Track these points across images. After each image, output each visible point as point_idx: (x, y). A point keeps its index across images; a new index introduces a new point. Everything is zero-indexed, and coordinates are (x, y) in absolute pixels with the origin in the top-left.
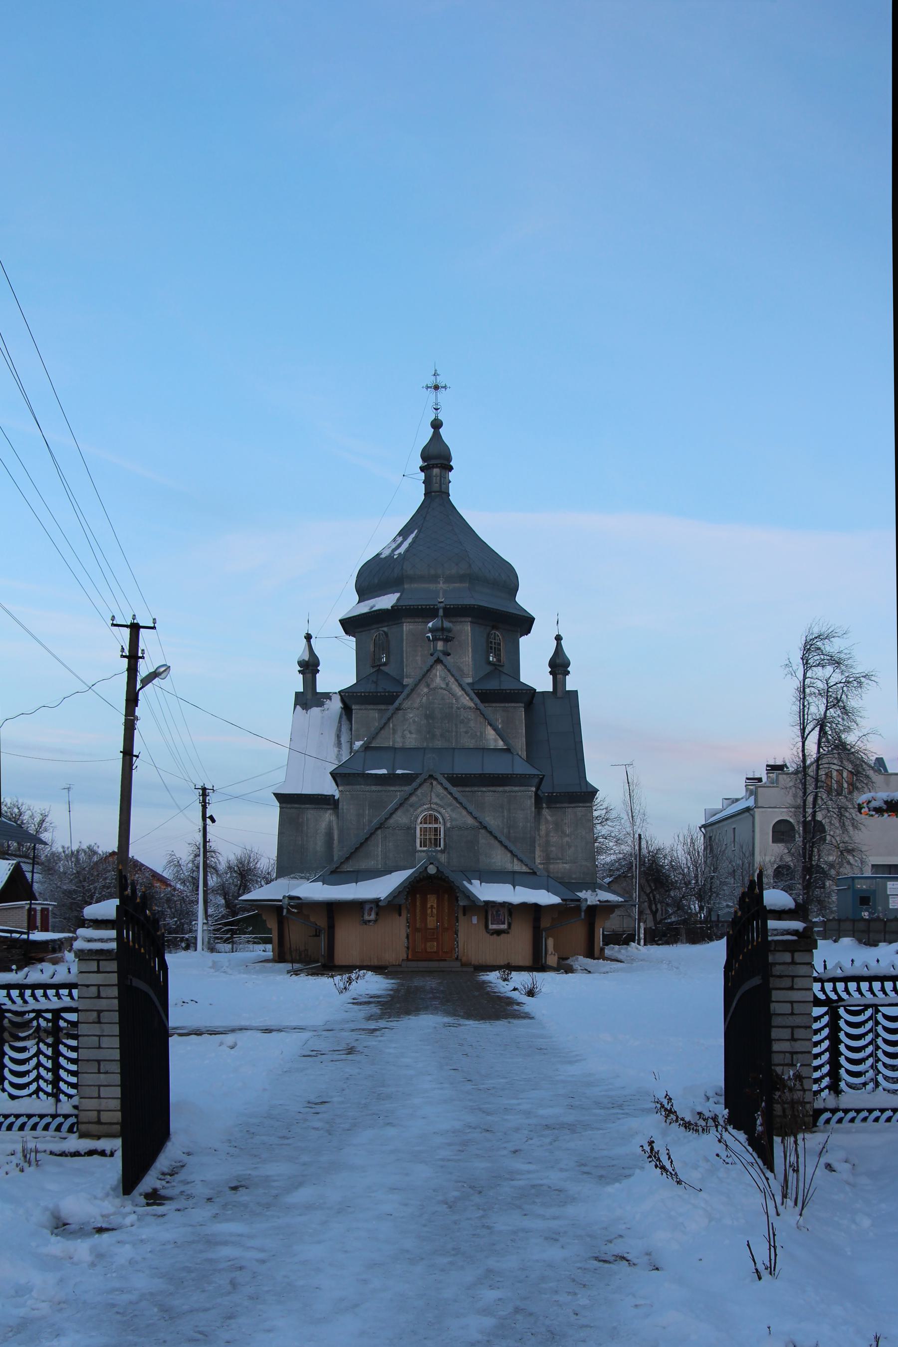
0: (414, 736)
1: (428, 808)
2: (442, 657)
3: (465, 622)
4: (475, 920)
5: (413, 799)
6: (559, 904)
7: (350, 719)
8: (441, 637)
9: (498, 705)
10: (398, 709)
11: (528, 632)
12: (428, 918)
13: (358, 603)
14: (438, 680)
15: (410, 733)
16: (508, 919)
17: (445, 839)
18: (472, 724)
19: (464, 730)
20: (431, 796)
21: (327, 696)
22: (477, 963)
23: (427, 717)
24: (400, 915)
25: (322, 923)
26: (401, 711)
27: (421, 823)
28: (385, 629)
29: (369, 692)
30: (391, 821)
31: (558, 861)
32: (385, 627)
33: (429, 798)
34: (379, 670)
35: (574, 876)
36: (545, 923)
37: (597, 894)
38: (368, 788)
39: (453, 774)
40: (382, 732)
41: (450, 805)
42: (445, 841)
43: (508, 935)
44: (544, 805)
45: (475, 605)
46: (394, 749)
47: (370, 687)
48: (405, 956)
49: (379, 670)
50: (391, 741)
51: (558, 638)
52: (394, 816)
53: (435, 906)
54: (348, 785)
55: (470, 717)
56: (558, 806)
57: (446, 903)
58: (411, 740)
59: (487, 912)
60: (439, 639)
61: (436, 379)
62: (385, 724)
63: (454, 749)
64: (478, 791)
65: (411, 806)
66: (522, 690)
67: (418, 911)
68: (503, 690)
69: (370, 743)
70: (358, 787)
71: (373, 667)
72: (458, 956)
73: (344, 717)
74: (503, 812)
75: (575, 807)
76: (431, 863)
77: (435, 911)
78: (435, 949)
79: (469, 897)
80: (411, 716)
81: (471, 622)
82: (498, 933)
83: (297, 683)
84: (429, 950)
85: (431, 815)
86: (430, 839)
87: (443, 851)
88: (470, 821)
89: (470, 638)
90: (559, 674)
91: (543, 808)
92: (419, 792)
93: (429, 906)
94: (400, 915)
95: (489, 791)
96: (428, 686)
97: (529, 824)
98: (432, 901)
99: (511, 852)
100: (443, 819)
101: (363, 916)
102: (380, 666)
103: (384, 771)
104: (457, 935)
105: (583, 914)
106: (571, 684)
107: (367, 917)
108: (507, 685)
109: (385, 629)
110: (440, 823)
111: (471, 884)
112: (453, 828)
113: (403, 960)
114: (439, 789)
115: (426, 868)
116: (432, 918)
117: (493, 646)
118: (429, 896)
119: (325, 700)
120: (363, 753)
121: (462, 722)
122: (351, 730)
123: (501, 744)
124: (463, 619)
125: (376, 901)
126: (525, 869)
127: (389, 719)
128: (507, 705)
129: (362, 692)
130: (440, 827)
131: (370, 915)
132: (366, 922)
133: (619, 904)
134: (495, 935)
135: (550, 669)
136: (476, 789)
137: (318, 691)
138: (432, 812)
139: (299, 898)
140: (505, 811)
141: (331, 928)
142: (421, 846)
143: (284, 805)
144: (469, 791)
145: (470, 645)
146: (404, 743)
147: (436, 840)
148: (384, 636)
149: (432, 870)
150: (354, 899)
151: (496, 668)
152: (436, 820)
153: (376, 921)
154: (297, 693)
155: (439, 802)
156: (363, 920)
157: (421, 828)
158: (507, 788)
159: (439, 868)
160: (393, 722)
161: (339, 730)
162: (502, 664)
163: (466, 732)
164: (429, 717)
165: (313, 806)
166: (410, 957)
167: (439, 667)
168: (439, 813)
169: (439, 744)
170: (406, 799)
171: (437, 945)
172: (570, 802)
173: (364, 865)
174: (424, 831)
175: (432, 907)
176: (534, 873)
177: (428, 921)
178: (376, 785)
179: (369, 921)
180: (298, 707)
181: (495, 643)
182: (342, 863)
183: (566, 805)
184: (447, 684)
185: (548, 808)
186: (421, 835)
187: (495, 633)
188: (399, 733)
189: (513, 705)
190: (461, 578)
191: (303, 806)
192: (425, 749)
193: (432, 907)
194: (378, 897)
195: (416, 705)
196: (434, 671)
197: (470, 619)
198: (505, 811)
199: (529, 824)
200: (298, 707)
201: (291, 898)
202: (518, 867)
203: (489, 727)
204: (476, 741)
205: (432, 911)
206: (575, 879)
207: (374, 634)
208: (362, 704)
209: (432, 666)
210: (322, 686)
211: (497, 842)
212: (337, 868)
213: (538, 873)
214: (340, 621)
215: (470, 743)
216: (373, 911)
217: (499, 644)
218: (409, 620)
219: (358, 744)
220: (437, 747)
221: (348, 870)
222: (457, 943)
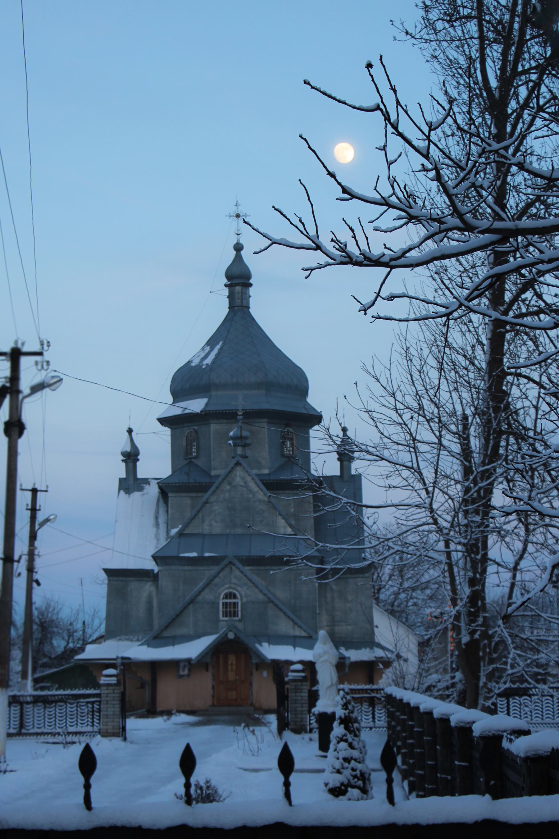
0: (219, 524)
2: (241, 460)
4: (265, 674)
5: (217, 580)
7: (166, 501)
10: (206, 503)
14: (238, 479)
15: (216, 522)
21: (146, 481)
24: (207, 670)
25: (147, 677)
27: (223, 599)
29: (183, 483)
30: (200, 598)
38: (181, 568)
46: (203, 535)
47: (182, 479)
48: (211, 703)
49: (190, 462)
52: (202, 593)
53: (234, 663)
58: (218, 528)
60: (239, 446)
62: (196, 515)
69: (184, 530)
70: (174, 567)
71: (186, 459)
73: (161, 501)
76: (231, 631)
77: (234, 667)
85: (231, 593)
87: (240, 621)
88: (261, 597)
92: (221, 575)
93: (230, 663)
94: (207, 670)
96: (230, 484)
98: (232, 659)
99: (293, 621)
100: (241, 596)
101: (178, 671)
102: (191, 458)
103: (194, 554)
107: (181, 673)
111: (261, 645)
114: (237, 573)
115: (226, 635)
119: (144, 485)
122: (167, 512)
125: (189, 661)
126: (304, 634)
127: (198, 511)
129: (176, 483)
132: (181, 677)
137: (139, 476)
139: (129, 659)
141: (154, 681)
142: (223, 616)
149: (231, 636)
152: (235, 597)
153: (188, 675)
154: (121, 480)
157: (223, 603)
161: (157, 512)
163: (262, 521)
166: (215, 703)
167: (239, 468)
169: (239, 531)
170: (212, 580)
174: (225, 605)
175: (232, 664)
178: (188, 565)
179: (183, 676)
180: (122, 492)
182: (162, 631)
184: (246, 483)
186: (223, 608)
188: (207, 522)
192: (227, 535)
193: (232, 664)
201: (123, 658)
202: (298, 632)
203: (279, 517)
205: (232, 667)
208: (177, 492)
209: (233, 468)
210: (141, 474)
212: (158, 634)
219: (174, 531)
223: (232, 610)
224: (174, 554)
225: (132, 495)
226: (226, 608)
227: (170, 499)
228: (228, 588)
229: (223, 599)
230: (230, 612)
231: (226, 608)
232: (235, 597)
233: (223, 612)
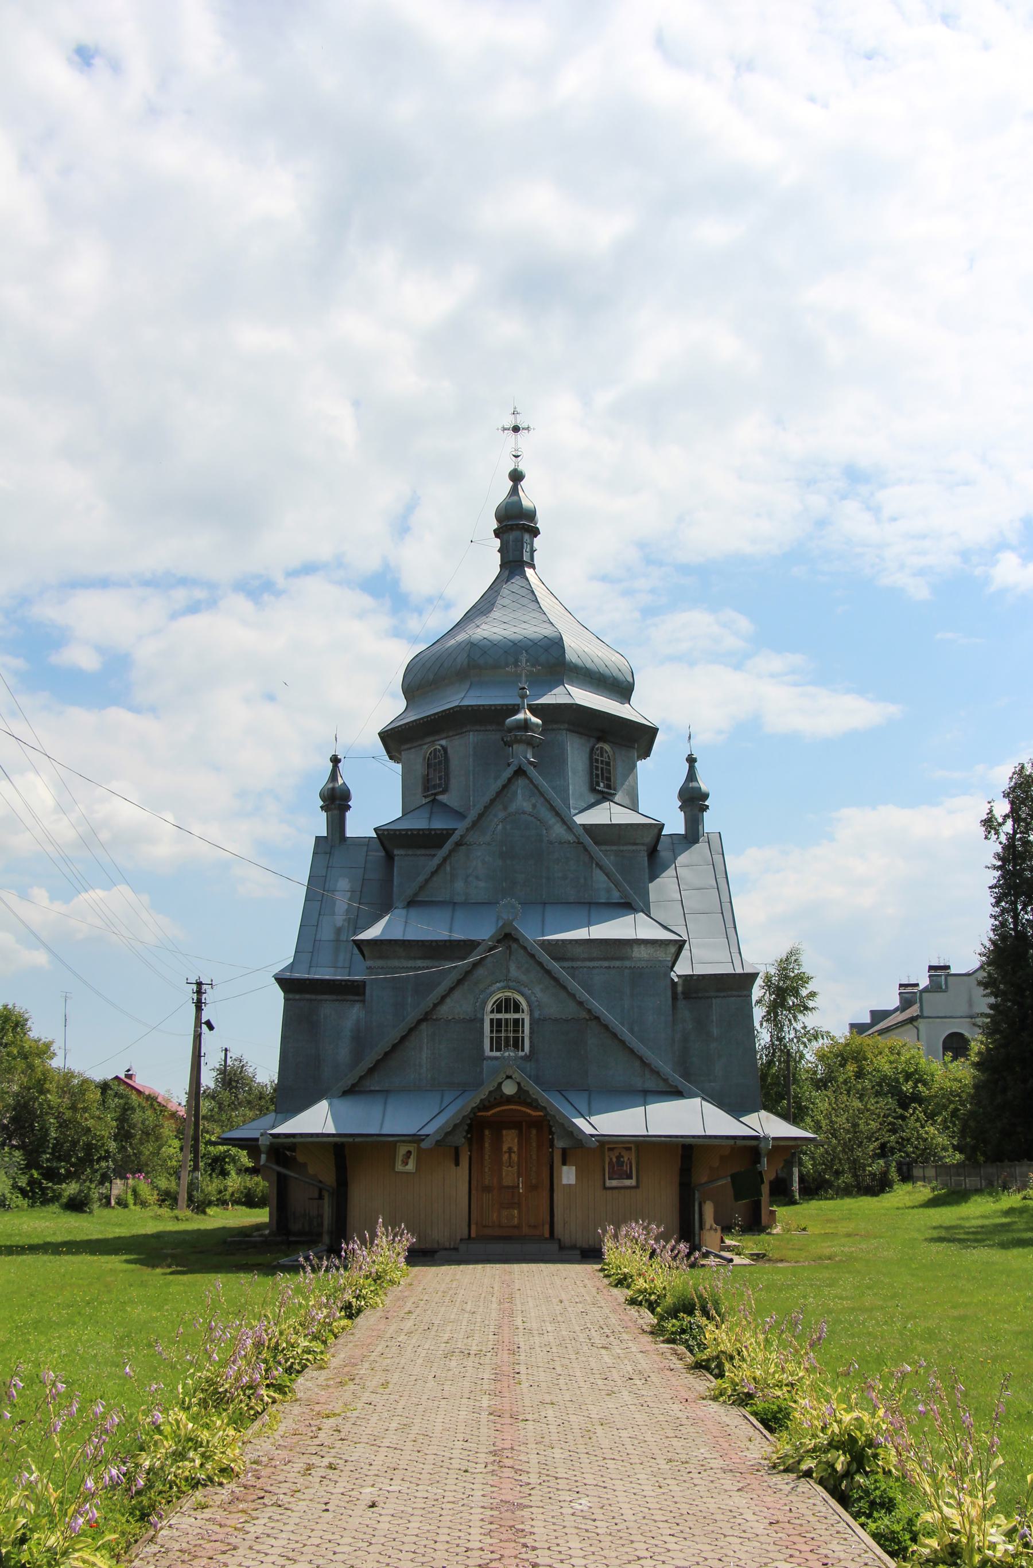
0: (482, 884)
11: (646, 753)
17: (531, 1038)
22: (585, 1246)
24: (457, 1164)
27: (492, 1012)
28: (443, 742)
30: (444, 1010)
32: (442, 739)
34: (434, 801)
40: (435, 879)
42: (531, 1042)
48: (465, 1235)
49: (434, 801)
51: (691, 760)
52: (448, 1000)
53: (515, 1149)
57: (534, 1144)
61: (516, 419)
71: (425, 797)
75: (724, 997)
76: (509, 1077)
77: (515, 1157)
78: (516, 1221)
79: (572, 1133)
81: (567, 730)
83: (319, 824)
85: (507, 1000)
86: (507, 1038)
87: (526, 1058)
93: (505, 1148)
94: (457, 1164)
100: (529, 1005)
106: (710, 822)
109: (443, 742)
110: (523, 1012)
112: (545, 1020)
113: (461, 1240)
115: (500, 1084)
117: (600, 765)
118: (504, 1132)
124: (555, 726)
130: (523, 1019)
131: (407, 1164)
137: (348, 834)
142: (491, 1050)
143: (291, 996)
147: (516, 1039)
148: (442, 752)
152: (517, 1008)
154: (318, 839)
157: (492, 1020)
159: (522, 1085)
160: (450, 863)
165: (334, 997)
166: (473, 1235)
167: (521, 782)
168: (523, 995)
171: (520, 1213)
174: (496, 1025)
175: (510, 1151)
177: (504, 1174)
185: (684, 998)
186: (492, 1031)
191: (319, 997)
193: (510, 1151)
205: (510, 1157)
207: (427, 750)
212: (353, 1086)
216: (412, 1157)
218: (478, 728)
221: (373, 1088)
227: (396, 858)
229: (492, 1012)
230: (507, 1038)
231: (499, 1031)
233: (492, 1038)
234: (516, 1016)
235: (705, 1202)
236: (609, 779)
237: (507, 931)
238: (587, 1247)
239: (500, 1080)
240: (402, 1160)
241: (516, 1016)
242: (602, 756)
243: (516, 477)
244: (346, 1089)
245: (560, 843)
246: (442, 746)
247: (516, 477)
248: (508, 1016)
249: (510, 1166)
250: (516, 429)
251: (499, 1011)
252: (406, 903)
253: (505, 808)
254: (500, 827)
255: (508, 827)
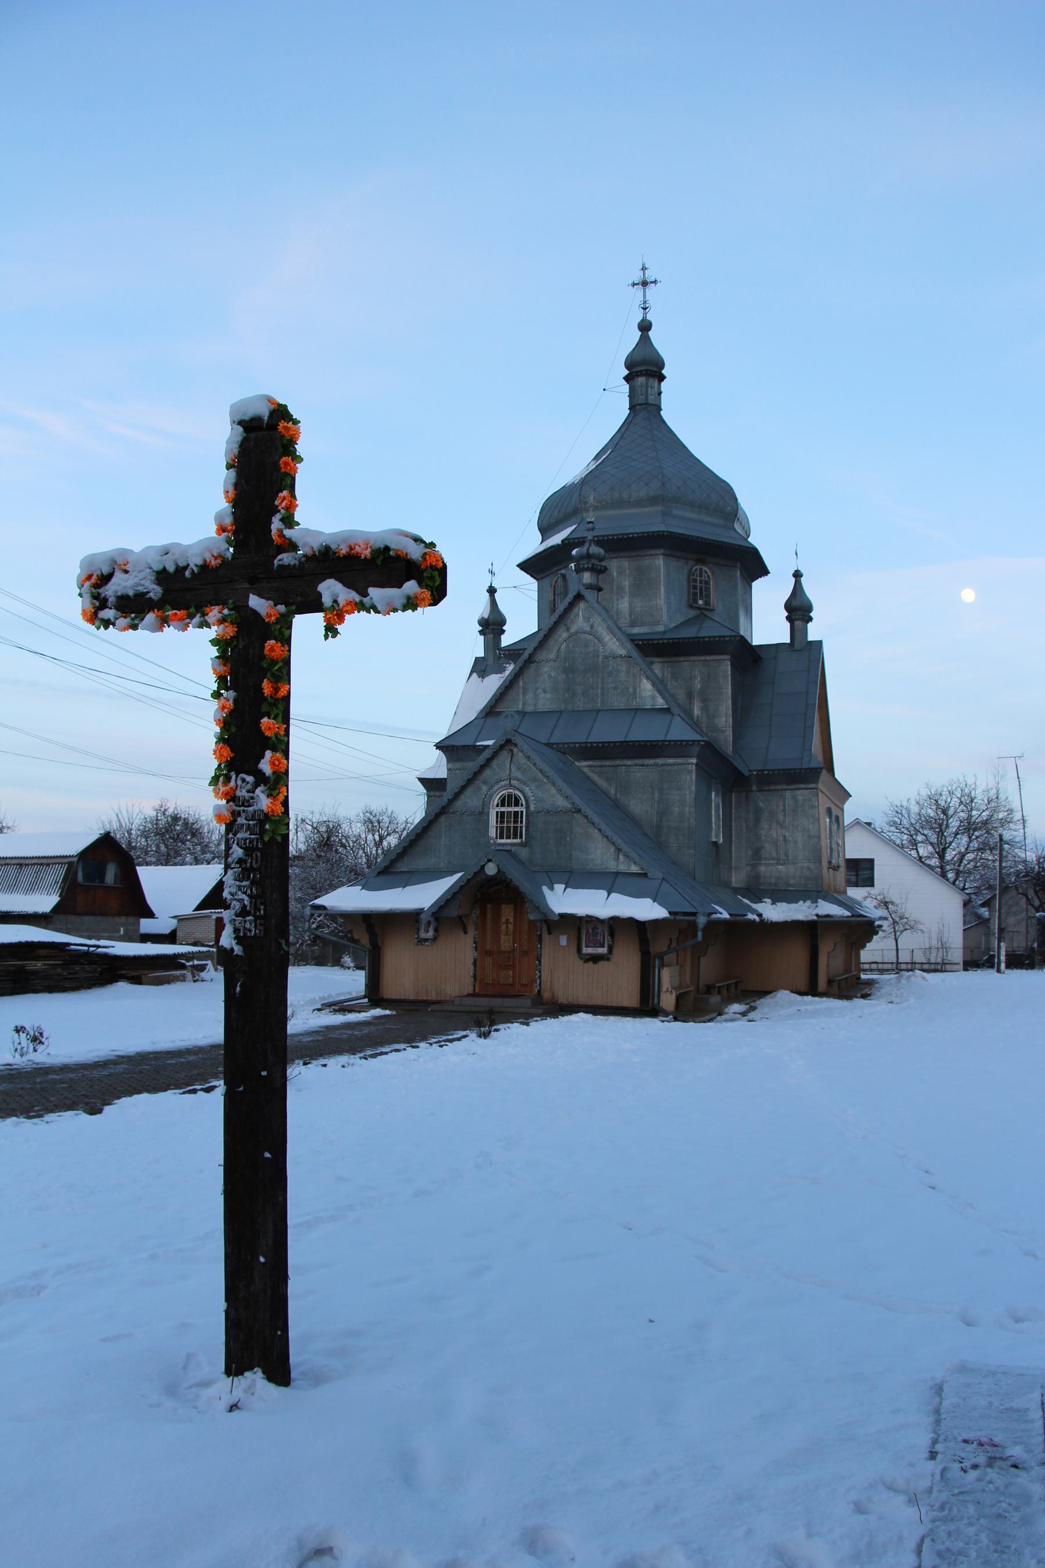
0: (549, 696)
1: (506, 785)
3: (656, 555)
4: (563, 940)
6: (664, 920)
8: (586, 566)
9: (696, 658)
12: (502, 937)
13: (541, 543)
15: (545, 691)
16: (608, 941)
18: (623, 676)
19: (613, 685)
20: (510, 769)
22: (565, 1002)
23: (566, 670)
24: (466, 933)
26: (534, 664)
27: (497, 806)
28: (563, 571)
30: (458, 804)
31: (771, 862)
32: (563, 568)
33: (508, 772)
35: (792, 882)
36: (659, 946)
37: (817, 906)
39: (587, 743)
41: (535, 780)
43: (609, 962)
44: (754, 788)
45: (664, 531)
50: (521, 703)
51: (797, 575)
52: (462, 797)
53: (512, 920)
54: (457, 761)
55: (620, 668)
56: (772, 788)
59: (579, 930)
63: (599, 711)
64: (622, 766)
65: (485, 783)
66: (724, 637)
67: (489, 926)
68: (700, 638)
72: (539, 991)
74: (653, 793)
76: (489, 861)
77: (511, 927)
80: (546, 670)
81: (663, 554)
82: (595, 959)
84: (502, 981)
85: (510, 796)
86: (509, 828)
87: (522, 845)
89: (662, 574)
90: (798, 620)
91: (751, 791)
93: (503, 920)
94: (466, 933)
95: (637, 765)
97: (687, 809)
100: (526, 801)
101: (418, 934)
104: (540, 962)
105: (700, 934)
106: (813, 632)
107: (423, 935)
108: (709, 631)
110: (522, 805)
111: (552, 889)
115: (483, 867)
116: (507, 937)
117: (698, 585)
118: (503, 906)
120: (484, 720)
121: (610, 674)
123: (660, 702)
124: (653, 552)
126: (634, 869)
128: (708, 658)
130: (522, 812)
131: (428, 932)
132: (422, 941)
133: (844, 919)
134: (590, 963)
135: (787, 614)
136: (618, 762)
138: (512, 791)
140: (656, 792)
143: (432, 793)
144: (609, 766)
145: (662, 583)
146: (536, 705)
147: (515, 828)
149: (491, 870)
150: (391, 910)
151: (702, 613)
153: (435, 939)
155: (520, 776)
156: (418, 938)
157: (497, 812)
158: (660, 761)
160: (523, 678)
162: (711, 608)
163: (615, 688)
164: (569, 669)
166: (477, 990)
169: (581, 703)
171: (513, 972)
172: (788, 783)
173: (420, 863)
175: (507, 922)
176: (645, 875)
179: (426, 940)
180: (475, 675)
181: (701, 582)
183: (784, 787)
184: (592, 627)
185: (759, 791)
187: (701, 569)
189: (716, 657)
190: (653, 501)
194: (422, 907)
195: (552, 656)
196: (575, 610)
197: (662, 551)
198: (656, 792)
199: (687, 809)
200: (475, 675)
204: (628, 700)
206: (793, 885)
211: (596, 831)
213: (649, 875)
214: (518, 566)
215: (619, 702)
217: (707, 583)
220: (578, 709)
221: (402, 870)
222: (540, 972)
223: (512, 825)
224: (469, 742)
225: (487, 679)
226: (502, 822)
228: (505, 787)
230: (509, 828)
231: (502, 822)
232: (517, 804)
234: (517, 809)
235: (663, 969)
236: (708, 596)
237: (509, 737)
238: (567, 1003)
239: (483, 863)
240: (424, 929)
241: (517, 809)
242: (701, 576)
243: (645, 327)
244: (380, 870)
245: (614, 658)
246: (562, 574)
247: (645, 327)
248: (510, 809)
249: (507, 934)
250: (645, 284)
251: (503, 805)
252: (484, 714)
253: (568, 629)
254: (563, 646)
255: (571, 645)
